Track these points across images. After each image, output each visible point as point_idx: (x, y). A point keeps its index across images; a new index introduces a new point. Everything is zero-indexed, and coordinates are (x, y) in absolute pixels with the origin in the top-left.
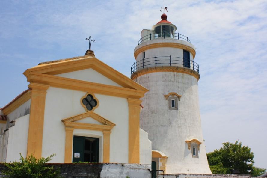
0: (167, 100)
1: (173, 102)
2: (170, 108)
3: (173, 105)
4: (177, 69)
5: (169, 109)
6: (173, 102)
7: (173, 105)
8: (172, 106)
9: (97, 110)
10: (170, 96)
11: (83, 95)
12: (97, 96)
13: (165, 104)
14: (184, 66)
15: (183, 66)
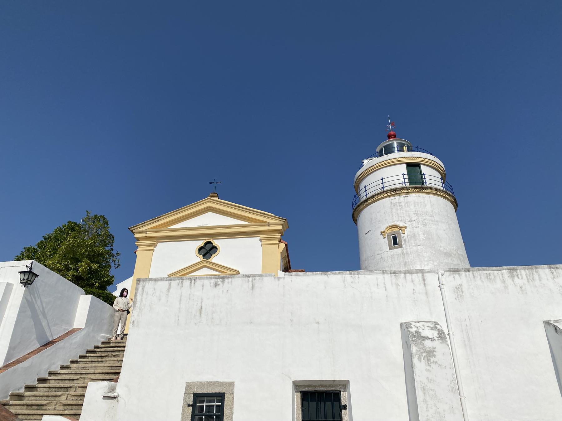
0: (384, 238)
1: (395, 239)
2: (391, 248)
3: (395, 243)
4: (395, 191)
5: (390, 249)
6: (395, 239)
7: (395, 243)
8: (397, 244)
9: (215, 259)
10: (389, 231)
11: (201, 243)
12: (216, 242)
13: (384, 242)
14: (409, 185)
15: (409, 185)
